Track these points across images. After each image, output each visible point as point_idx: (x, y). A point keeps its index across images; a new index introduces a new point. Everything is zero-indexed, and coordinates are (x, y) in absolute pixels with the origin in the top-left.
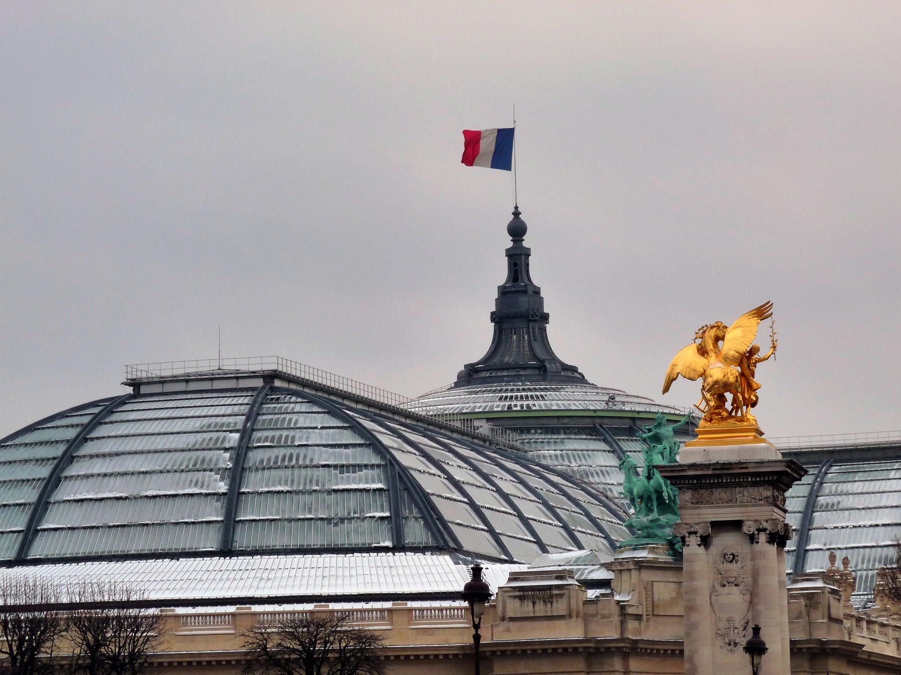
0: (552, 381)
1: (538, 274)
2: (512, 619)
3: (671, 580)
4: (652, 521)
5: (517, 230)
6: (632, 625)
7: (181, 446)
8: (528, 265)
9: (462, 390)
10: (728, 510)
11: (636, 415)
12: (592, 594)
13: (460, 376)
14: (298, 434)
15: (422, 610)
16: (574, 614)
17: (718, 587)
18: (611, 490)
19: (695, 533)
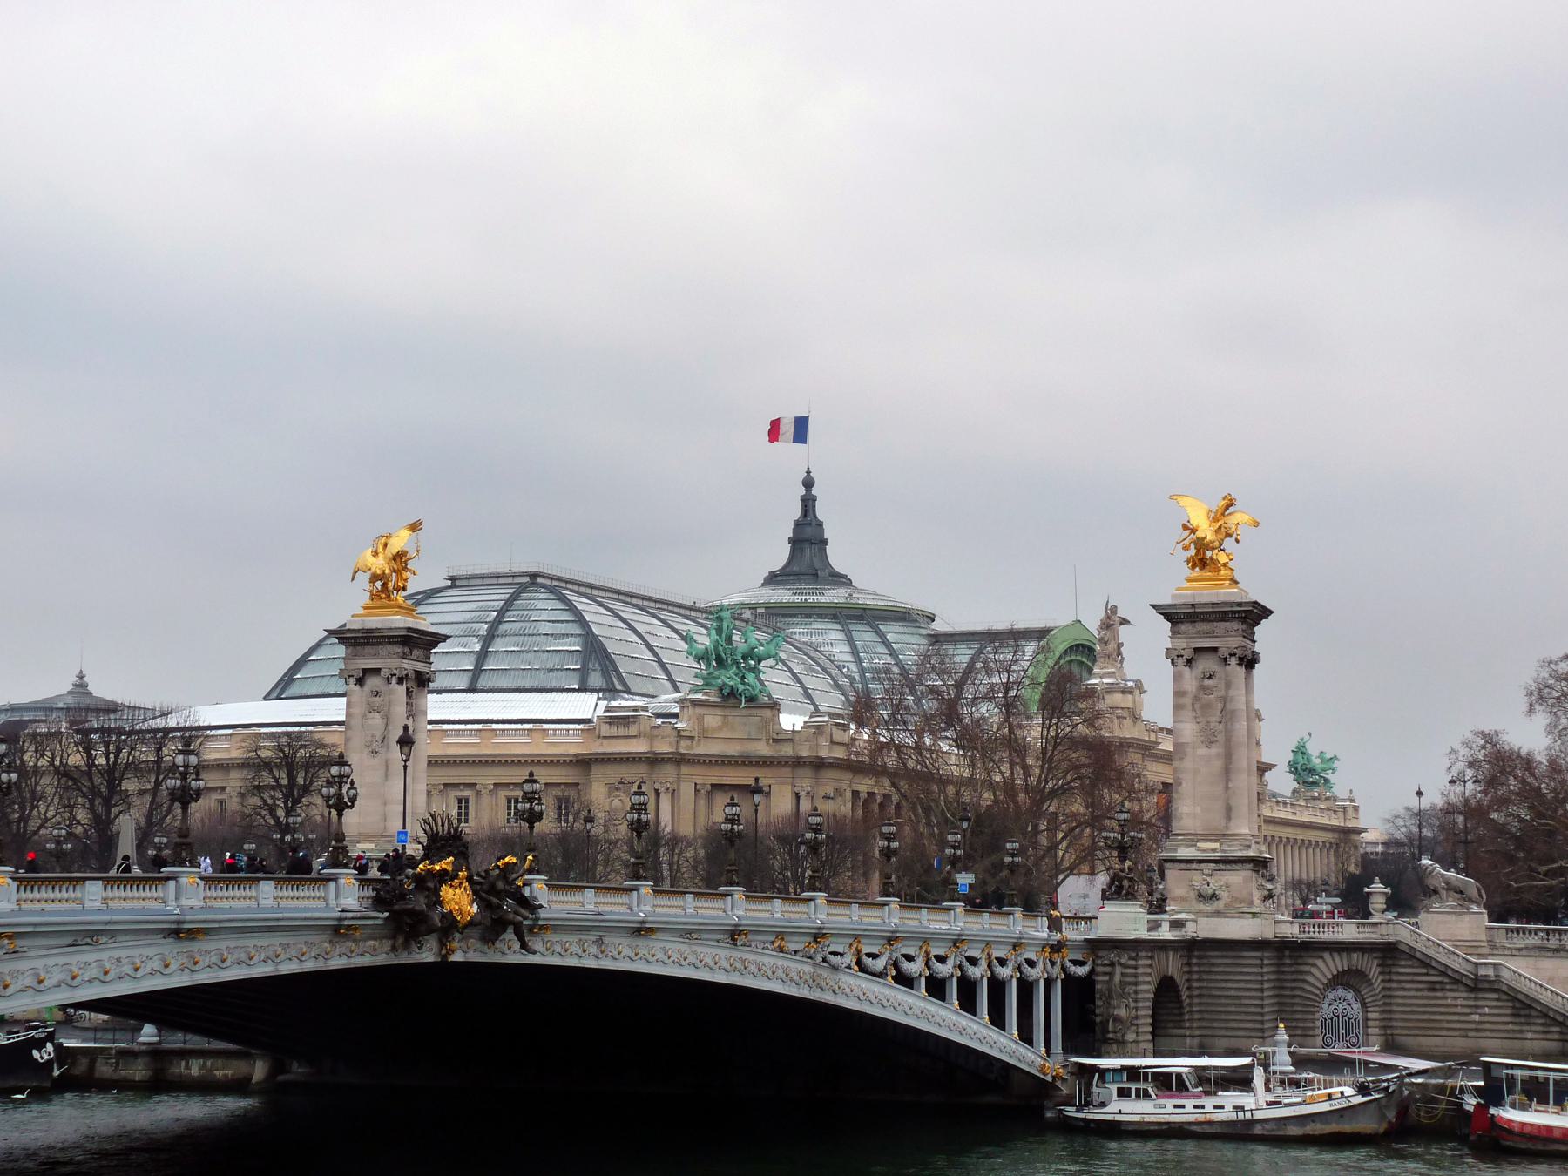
0: (820, 584)
1: (821, 512)
2: (605, 737)
3: (719, 714)
4: (709, 674)
5: (808, 483)
6: (683, 743)
7: (461, 620)
8: (815, 506)
9: (768, 588)
10: (374, 661)
11: (865, 607)
12: (659, 721)
13: (766, 579)
14: (535, 613)
15: (555, 730)
16: (642, 735)
17: (368, 714)
18: (834, 656)
19: (353, 676)
